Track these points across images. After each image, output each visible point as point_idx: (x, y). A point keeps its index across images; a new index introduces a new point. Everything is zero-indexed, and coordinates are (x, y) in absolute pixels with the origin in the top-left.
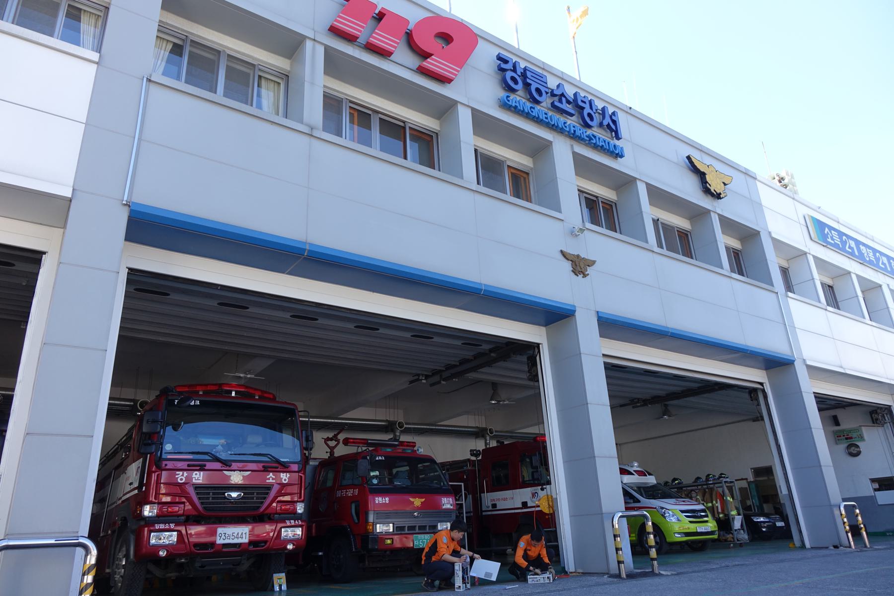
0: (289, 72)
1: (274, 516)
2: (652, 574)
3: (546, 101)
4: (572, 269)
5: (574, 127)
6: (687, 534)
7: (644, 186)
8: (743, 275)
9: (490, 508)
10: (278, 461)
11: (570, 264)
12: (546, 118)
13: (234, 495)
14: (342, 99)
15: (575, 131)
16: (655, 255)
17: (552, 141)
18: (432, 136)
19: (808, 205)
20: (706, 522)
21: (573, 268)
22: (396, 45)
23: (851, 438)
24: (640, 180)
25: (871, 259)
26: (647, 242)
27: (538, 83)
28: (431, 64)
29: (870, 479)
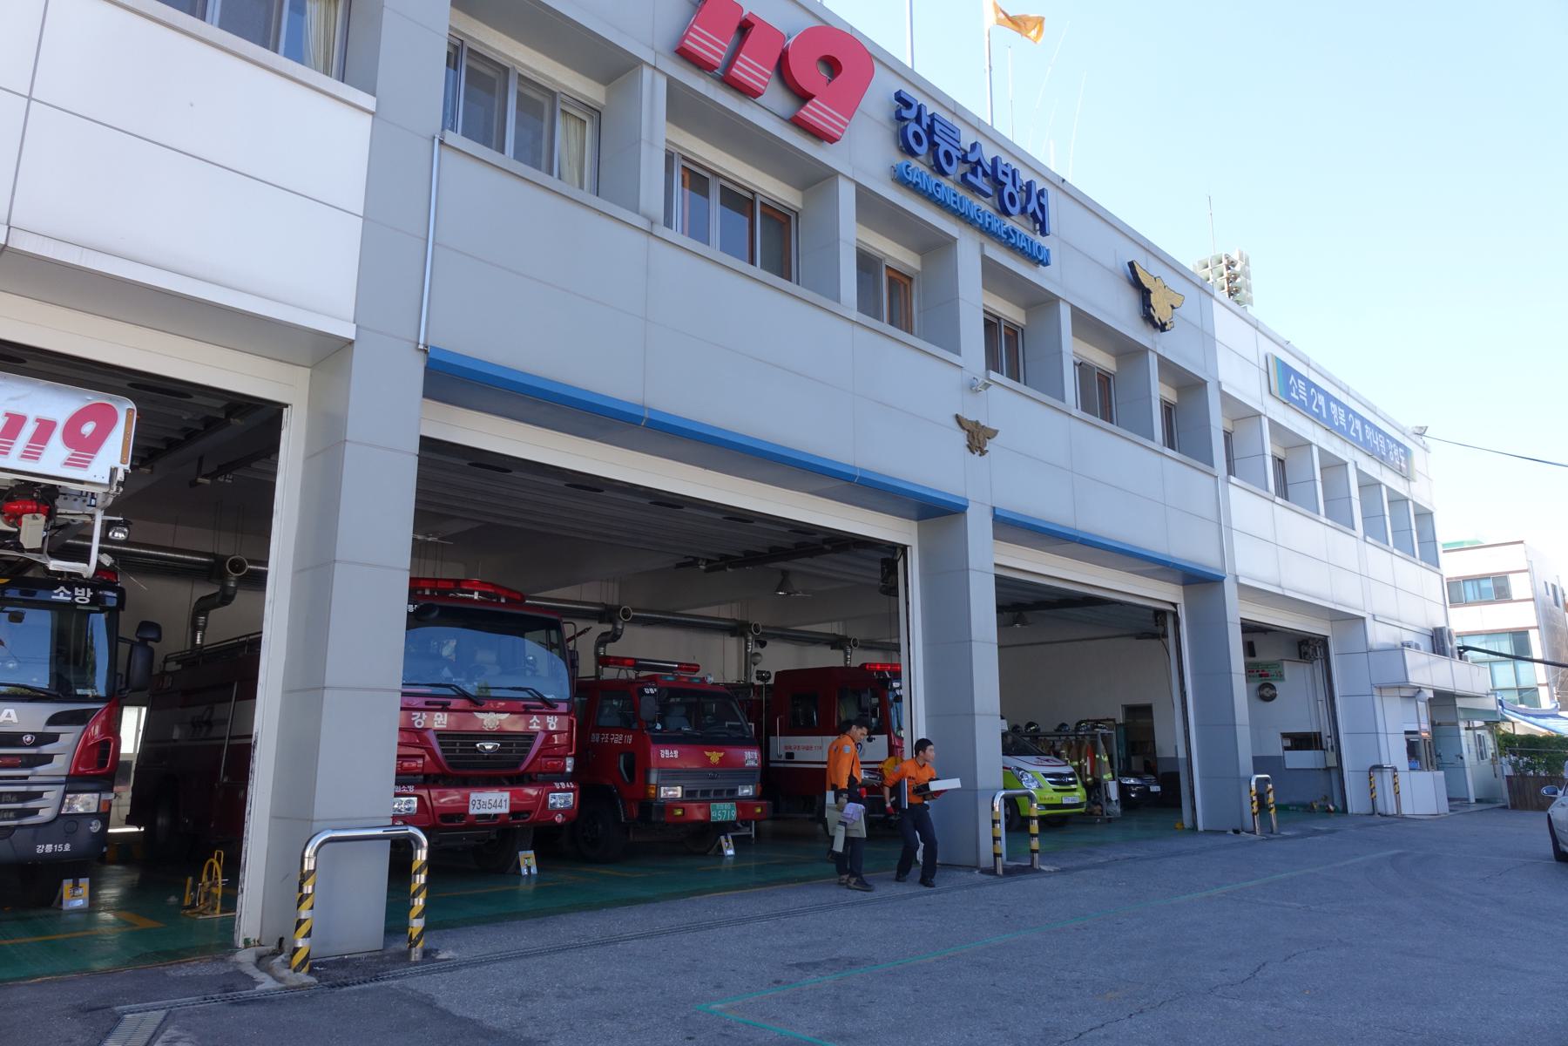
0: (603, 107)
1: (537, 776)
2: (1030, 870)
3: (956, 170)
4: (967, 443)
5: (989, 217)
6: (1049, 807)
7: (1068, 309)
8: (1174, 449)
9: (783, 758)
10: (543, 700)
11: (966, 437)
12: (955, 202)
13: (489, 746)
14: (673, 154)
15: (990, 224)
16: (1072, 420)
17: (957, 237)
18: (790, 217)
19: (1274, 338)
20: (1074, 790)
21: (968, 441)
22: (766, 80)
23: (1267, 675)
24: (1064, 300)
25: (1341, 423)
26: (1063, 400)
27: (945, 141)
28: (811, 112)
29: (1282, 734)
